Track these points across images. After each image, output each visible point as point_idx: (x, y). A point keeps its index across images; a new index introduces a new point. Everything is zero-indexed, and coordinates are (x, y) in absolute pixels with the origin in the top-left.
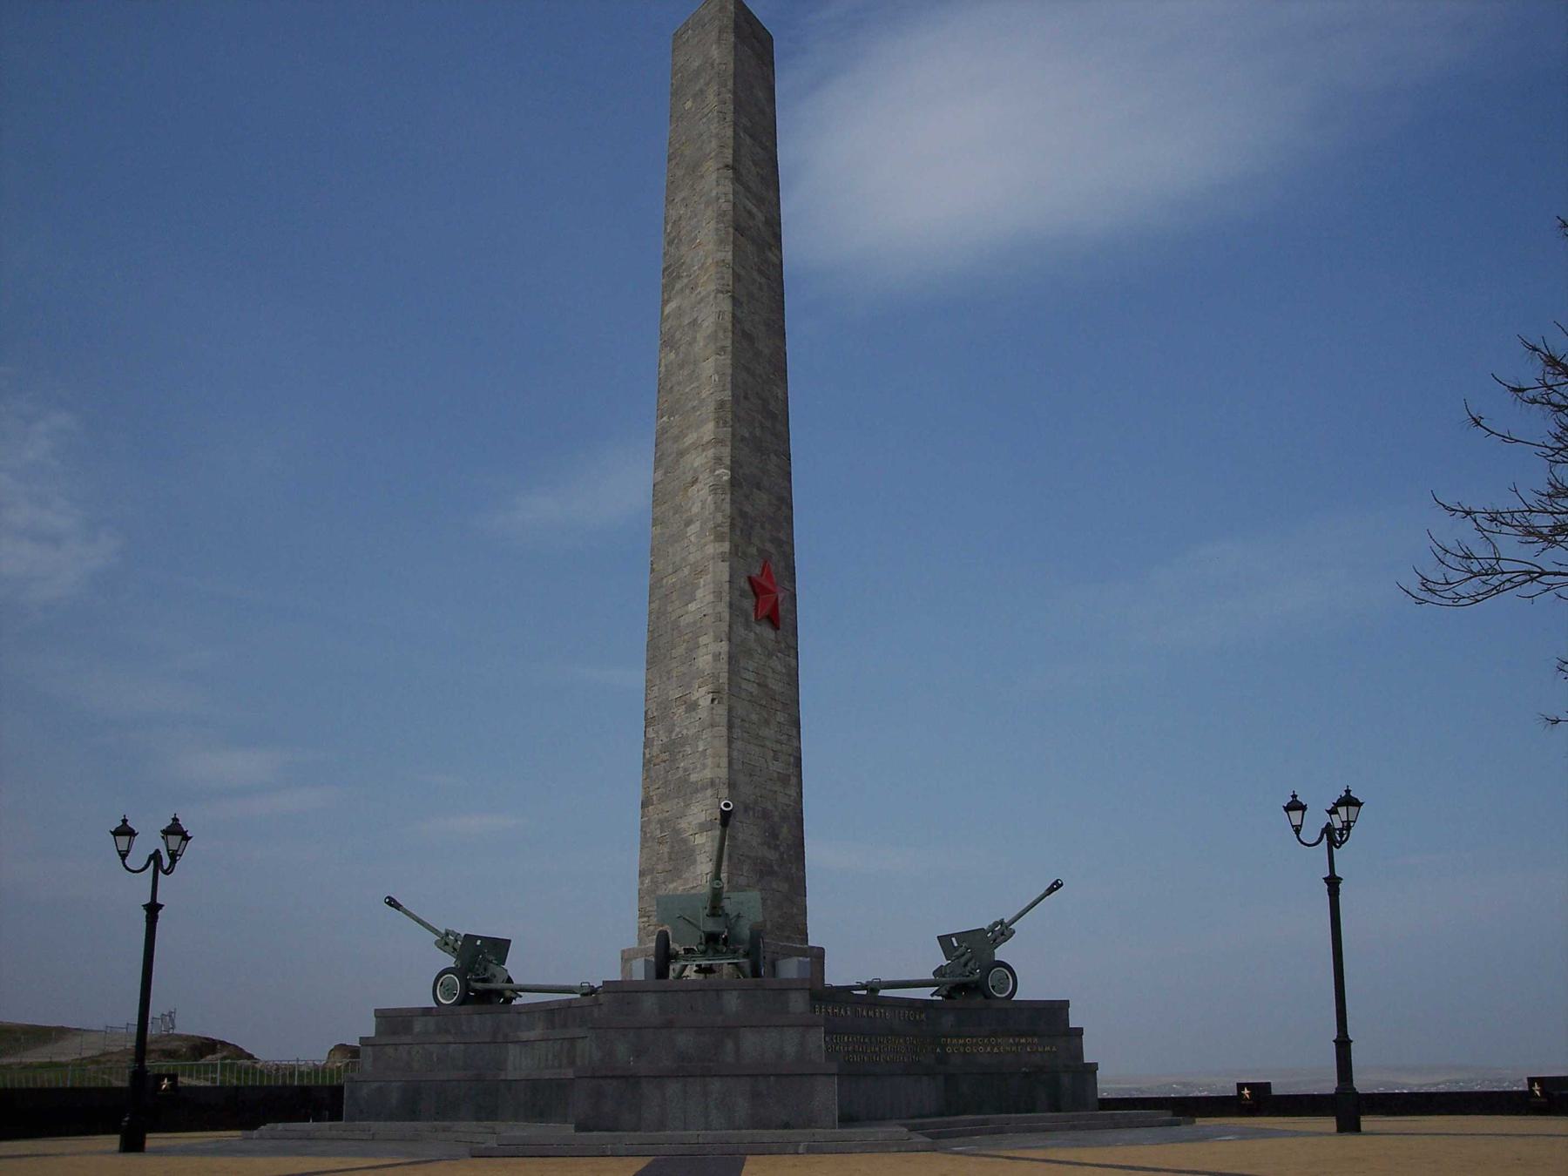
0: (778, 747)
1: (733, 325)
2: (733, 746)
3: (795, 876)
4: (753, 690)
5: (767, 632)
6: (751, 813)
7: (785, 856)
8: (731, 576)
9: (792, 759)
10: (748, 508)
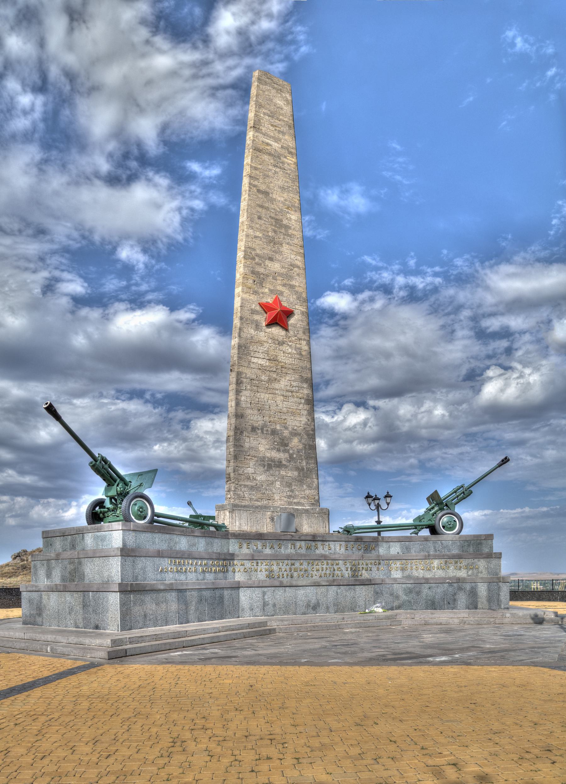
0: (290, 394)
1: (250, 187)
2: (241, 394)
3: (305, 467)
4: (263, 363)
5: (276, 331)
6: (260, 431)
7: (295, 456)
8: (242, 303)
9: (303, 401)
10: (262, 270)
